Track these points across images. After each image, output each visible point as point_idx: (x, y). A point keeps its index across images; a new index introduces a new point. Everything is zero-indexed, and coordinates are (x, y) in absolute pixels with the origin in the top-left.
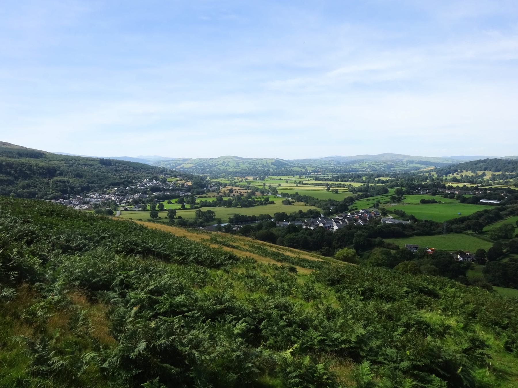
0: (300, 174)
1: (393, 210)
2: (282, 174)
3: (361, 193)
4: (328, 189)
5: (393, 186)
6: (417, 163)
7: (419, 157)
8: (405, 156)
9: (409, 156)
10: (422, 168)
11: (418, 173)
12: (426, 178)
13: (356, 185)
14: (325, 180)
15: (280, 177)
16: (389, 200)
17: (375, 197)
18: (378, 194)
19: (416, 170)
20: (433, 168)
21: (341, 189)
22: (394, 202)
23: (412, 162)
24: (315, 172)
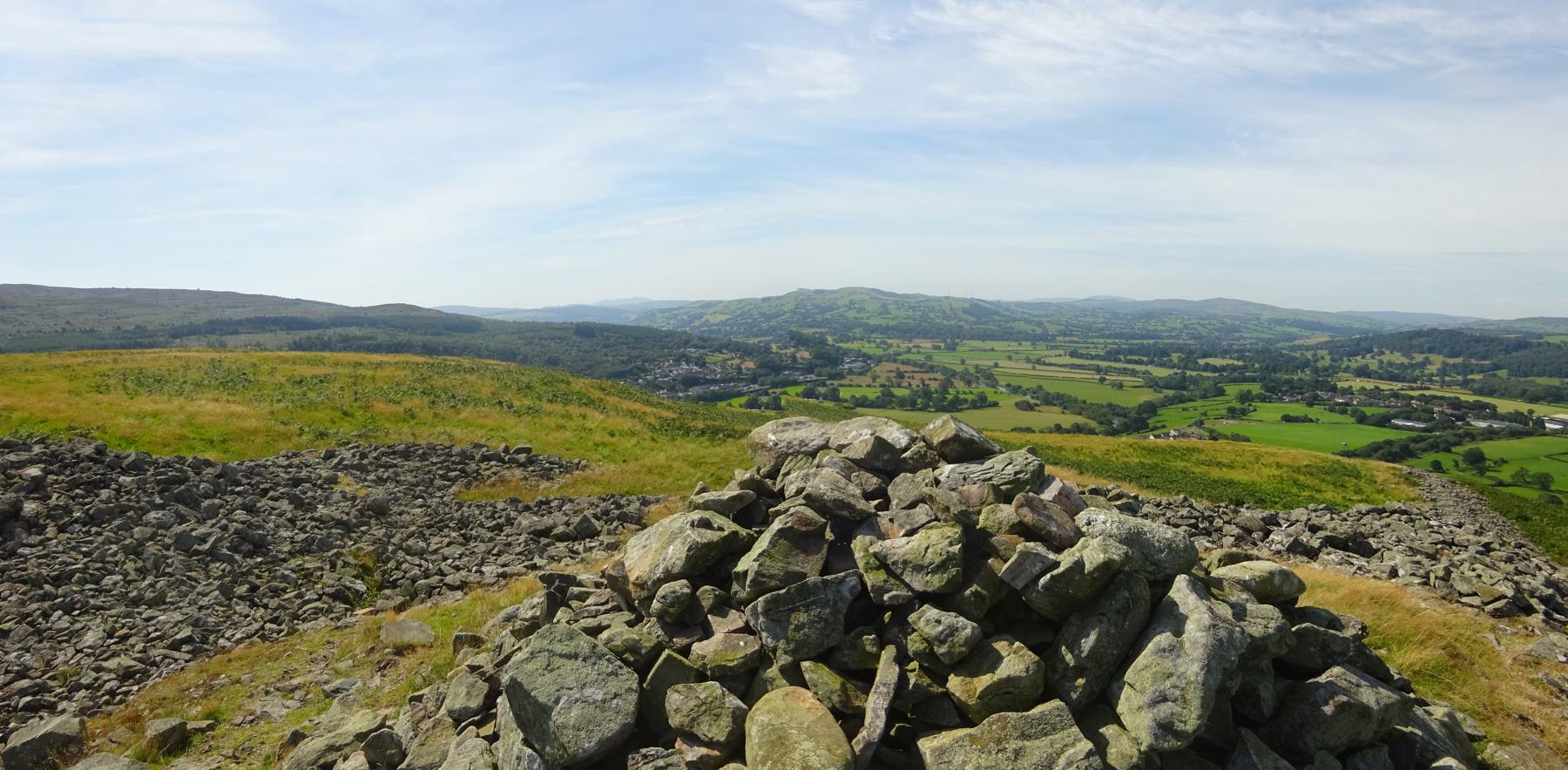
0: (1034, 339)
1: (1229, 434)
2: (993, 337)
3: (1171, 393)
4: (1102, 380)
5: (1235, 381)
6: (1290, 325)
7: (1296, 312)
8: (1264, 307)
9: (1272, 308)
10: (1301, 337)
11: (1292, 348)
12: (1305, 364)
13: (1161, 373)
14: (1093, 358)
15: (989, 344)
16: (1224, 412)
17: (1199, 403)
18: (1204, 397)
19: (1289, 340)
20: (1323, 338)
21: (1128, 380)
22: (1233, 418)
23: (1281, 322)
24: (1065, 335)
